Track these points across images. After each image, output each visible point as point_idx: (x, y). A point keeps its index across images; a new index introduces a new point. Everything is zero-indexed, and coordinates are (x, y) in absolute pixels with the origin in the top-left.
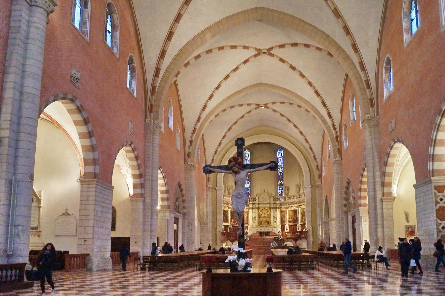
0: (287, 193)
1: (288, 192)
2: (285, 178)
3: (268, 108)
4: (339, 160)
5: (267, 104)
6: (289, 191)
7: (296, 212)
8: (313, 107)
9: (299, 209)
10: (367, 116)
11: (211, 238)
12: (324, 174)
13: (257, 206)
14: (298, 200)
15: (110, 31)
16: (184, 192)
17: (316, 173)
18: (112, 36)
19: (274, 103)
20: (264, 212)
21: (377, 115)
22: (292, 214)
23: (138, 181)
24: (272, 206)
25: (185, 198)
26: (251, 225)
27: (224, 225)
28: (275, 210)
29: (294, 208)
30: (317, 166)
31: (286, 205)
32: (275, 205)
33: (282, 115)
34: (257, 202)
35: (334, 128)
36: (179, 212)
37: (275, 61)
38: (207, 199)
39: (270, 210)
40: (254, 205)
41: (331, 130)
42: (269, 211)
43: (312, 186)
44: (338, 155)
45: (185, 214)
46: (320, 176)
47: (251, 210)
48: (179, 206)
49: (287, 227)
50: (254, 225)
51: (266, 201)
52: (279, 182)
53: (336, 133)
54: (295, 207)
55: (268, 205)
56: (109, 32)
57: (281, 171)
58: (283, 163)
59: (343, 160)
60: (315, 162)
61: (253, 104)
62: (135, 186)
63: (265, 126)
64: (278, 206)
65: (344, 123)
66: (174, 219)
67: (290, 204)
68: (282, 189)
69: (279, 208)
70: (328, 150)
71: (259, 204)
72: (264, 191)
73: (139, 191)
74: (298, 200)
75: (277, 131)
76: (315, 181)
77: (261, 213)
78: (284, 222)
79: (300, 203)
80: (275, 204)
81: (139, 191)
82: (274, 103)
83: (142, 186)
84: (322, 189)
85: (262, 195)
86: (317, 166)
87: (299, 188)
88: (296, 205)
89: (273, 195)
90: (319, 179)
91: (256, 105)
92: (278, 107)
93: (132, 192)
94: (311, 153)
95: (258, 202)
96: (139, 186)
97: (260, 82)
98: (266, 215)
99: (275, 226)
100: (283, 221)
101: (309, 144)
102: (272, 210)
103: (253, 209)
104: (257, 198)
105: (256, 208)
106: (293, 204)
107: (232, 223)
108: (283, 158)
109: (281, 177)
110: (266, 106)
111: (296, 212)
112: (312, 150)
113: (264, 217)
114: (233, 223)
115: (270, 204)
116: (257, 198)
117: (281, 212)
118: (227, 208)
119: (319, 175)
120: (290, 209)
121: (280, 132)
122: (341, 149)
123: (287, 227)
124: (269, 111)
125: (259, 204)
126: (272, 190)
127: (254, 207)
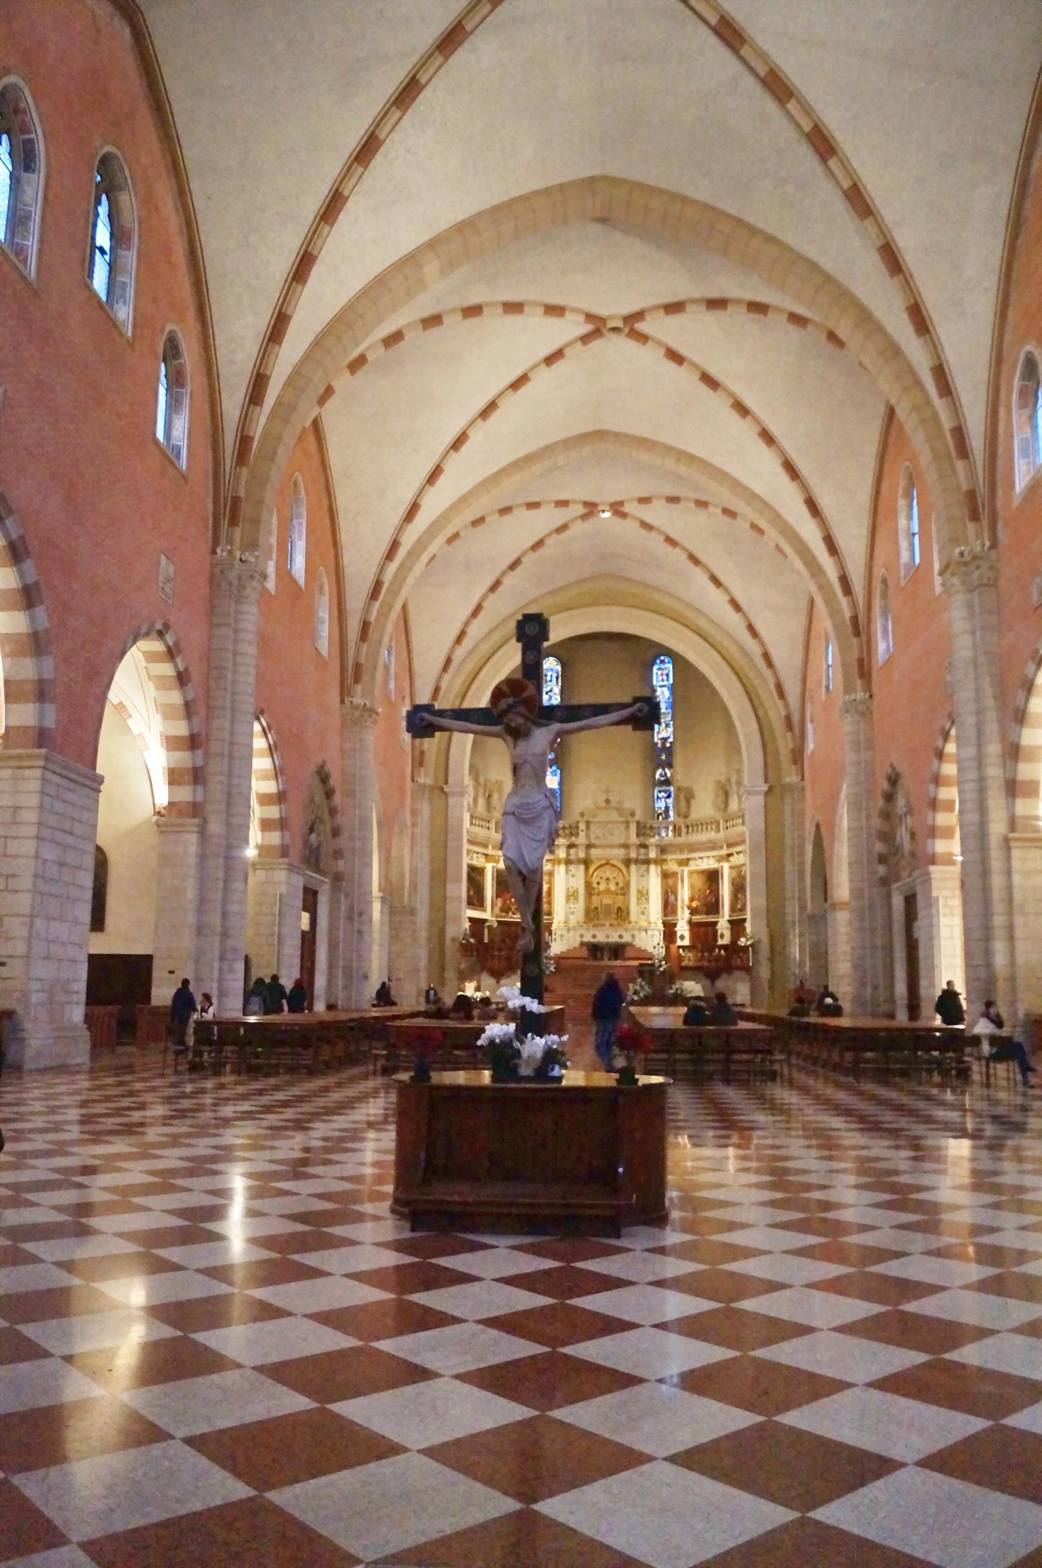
0: (684, 810)
1: (688, 806)
2: (678, 760)
3: (624, 515)
4: (862, 702)
5: (621, 503)
6: (693, 802)
7: (713, 877)
8: (778, 515)
9: (726, 866)
10: (957, 550)
11: (423, 963)
12: (810, 746)
13: (582, 855)
14: (721, 835)
15: (107, 248)
16: (337, 799)
17: (784, 744)
18: (112, 266)
19: (644, 500)
20: (608, 874)
21: (991, 548)
22: (700, 882)
23: (184, 758)
24: (633, 855)
25: (340, 819)
26: (562, 919)
27: (471, 919)
28: (644, 867)
29: (708, 863)
30: (788, 719)
31: (682, 851)
32: (642, 850)
33: (670, 541)
34: (581, 839)
35: (847, 590)
36: (318, 869)
37: (648, 357)
38: (414, 825)
40: (572, 851)
41: (835, 595)
42: (624, 870)
43: (771, 789)
44: (859, 682)
45: (337, 878)
46: (798, 755)
47: (563, 867)
48: (318, 848)
49: (683, 929)
50: (572, 917)
51: (612, 838)
52: (659, 771)
53: (854, 605)
55: (621, 852)
56: (102, 251)
57: (664, 735)
59: (876, 699)
60: (780, 703)
61: (575, 502)
62: (174, 777)
63: (614, 576)
64: (652, 854)
65: (879, 572)
66: (300, 894)
67: (692, 848)
68: (669, 796)
69: (656, 862)
70: (825, 667)
71: (589, 846)
72: (608, 801)
73: (185, 794)
74: (721, 835)
75: (656, 596)
76: (779, 769)
77: (595, 880)
78: (674, 912)
79: (729, 846)
80: (645, 846)
81: (185, 794)
82: (644, 500)
83: (197, 776)
84: (803, 799)
85: (602, 817)
86: (788, 719)
87: (726, 794)
88: (715, 853)
89: (637, 817)
90: (795, 762)
91: (586, 504)
92: (657, 514)
93: (162, 798)
94: (768, 673)
95: (586, 842)
96: (187, 778)
97: (599, 426)
98: (613, 887)
99: (644, 924)
100: (669, 907)
101: (762, 644)
102: (633, 867)
103: (568, 862)
104: (582, 826)
105: (579, 861)
106: (705, 850)
107: (497, 910)
109: (661, 756)
110: (618, 509)
111: (713, 877)
112: (770, 664)
113: (607, 891)
114: (502, 910)
115: (626, 846)
116: (582, 826)
117: (665, 876)
118: (482, 859)
119: (793, 750)
120: (693, 866)
121: (666, 601)
122: (870, 663)
123: (683, 929)
124: (629, 527)
125: (589, 846)
126: (631, 796)
127: (572, 857)
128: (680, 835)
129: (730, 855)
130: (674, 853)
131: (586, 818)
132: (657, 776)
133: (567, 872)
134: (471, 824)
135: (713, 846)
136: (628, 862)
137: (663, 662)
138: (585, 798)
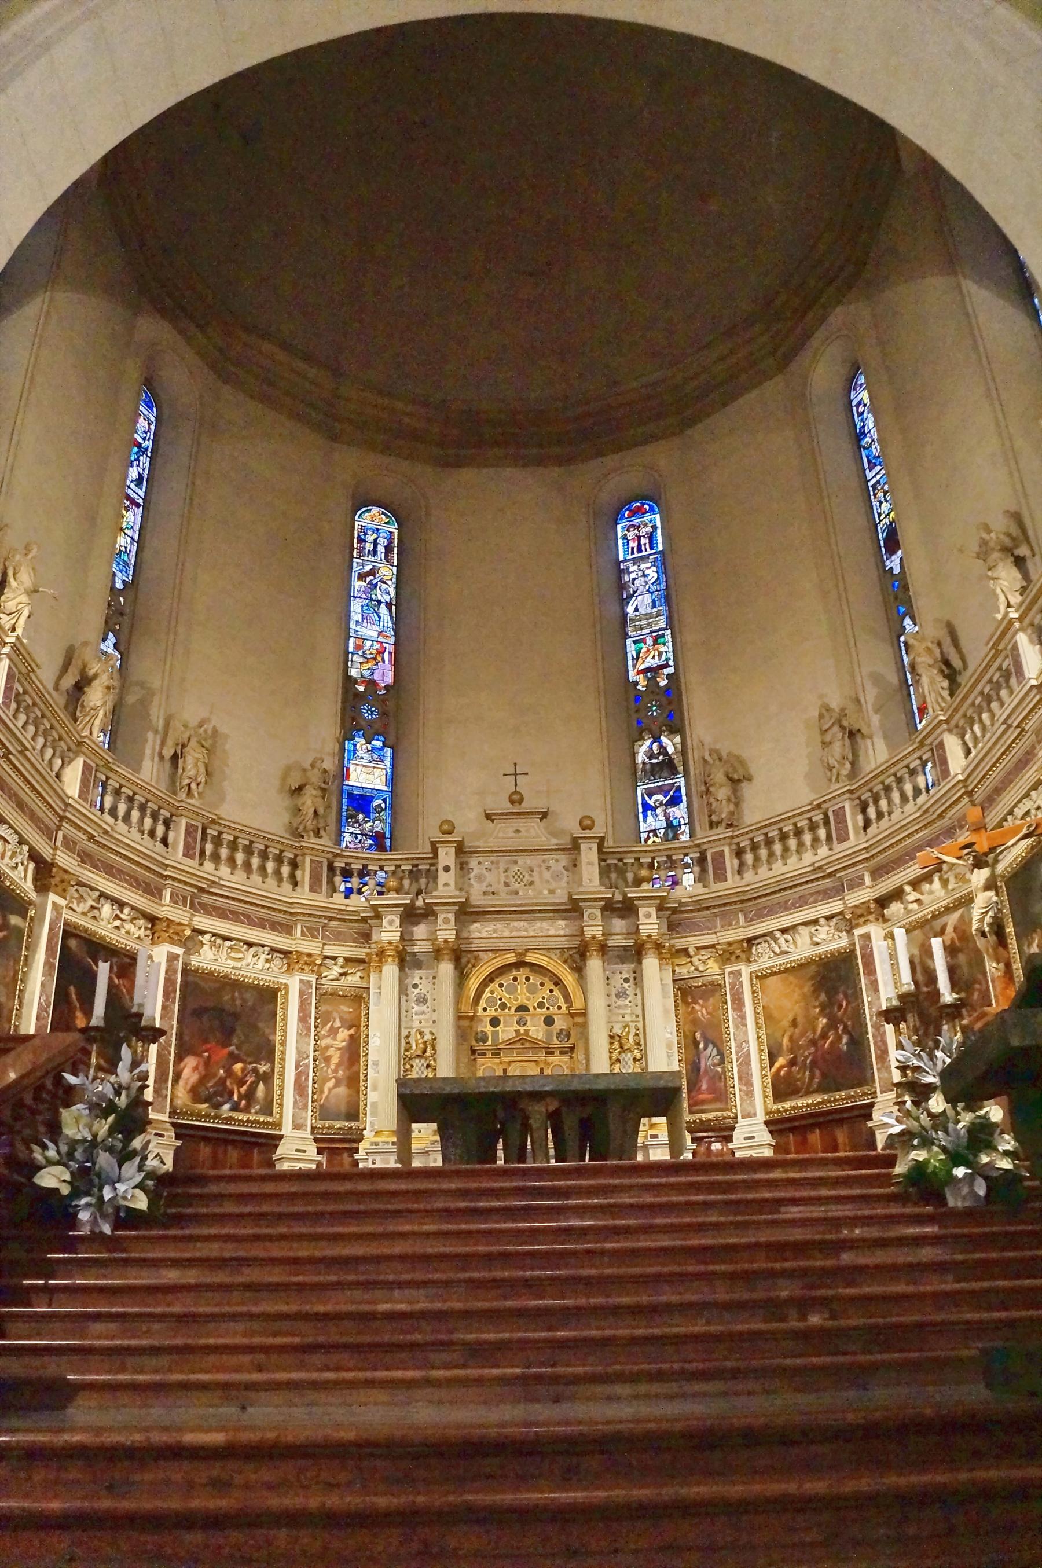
0: (725, 811)
1: (737, 800)
14: (855, 841)
20: (522, 996)
22: (791, 1001)
24: (594, 929)
28: (627, 969)
32: (619, 925)
34: (446, 887)
39: (579, 970)
40: (420, 931)
42: (569, 979)
47: (391, 970)
51: (527, 888)
54: (824, 932)
55: (558, 929)
57: (651, 662)
58: (668, 598)
68: (675, 801)
72: (516, 798)
74: (855, 841)
77: (485, 1011)
79: (878, 873)
85: (502, 834)
88: (834, 906)
89: (598, 831)
98: (537, 1031)
102: (594, 965)
103: (406, 960)
104: (447, 857)
105: (437, 954)
106: (802, 902)
108: (663, 562)
113: (522, 1043)
115: (573, 909)
116: (447, 857)
117: (686, 992)
118: (138, 929)
120: (765, 958)
125: (466, 913)
126: (576, 785)
128: (720, 875)
129: (883, 902)
130: (710, 929)
131: (456, 837)
132: (641, 758)
133: (403, 990)
134: (83, 794)
135: (831, 881)
136: (577, 957)
137: (634, 513)
138: (458, 793)
